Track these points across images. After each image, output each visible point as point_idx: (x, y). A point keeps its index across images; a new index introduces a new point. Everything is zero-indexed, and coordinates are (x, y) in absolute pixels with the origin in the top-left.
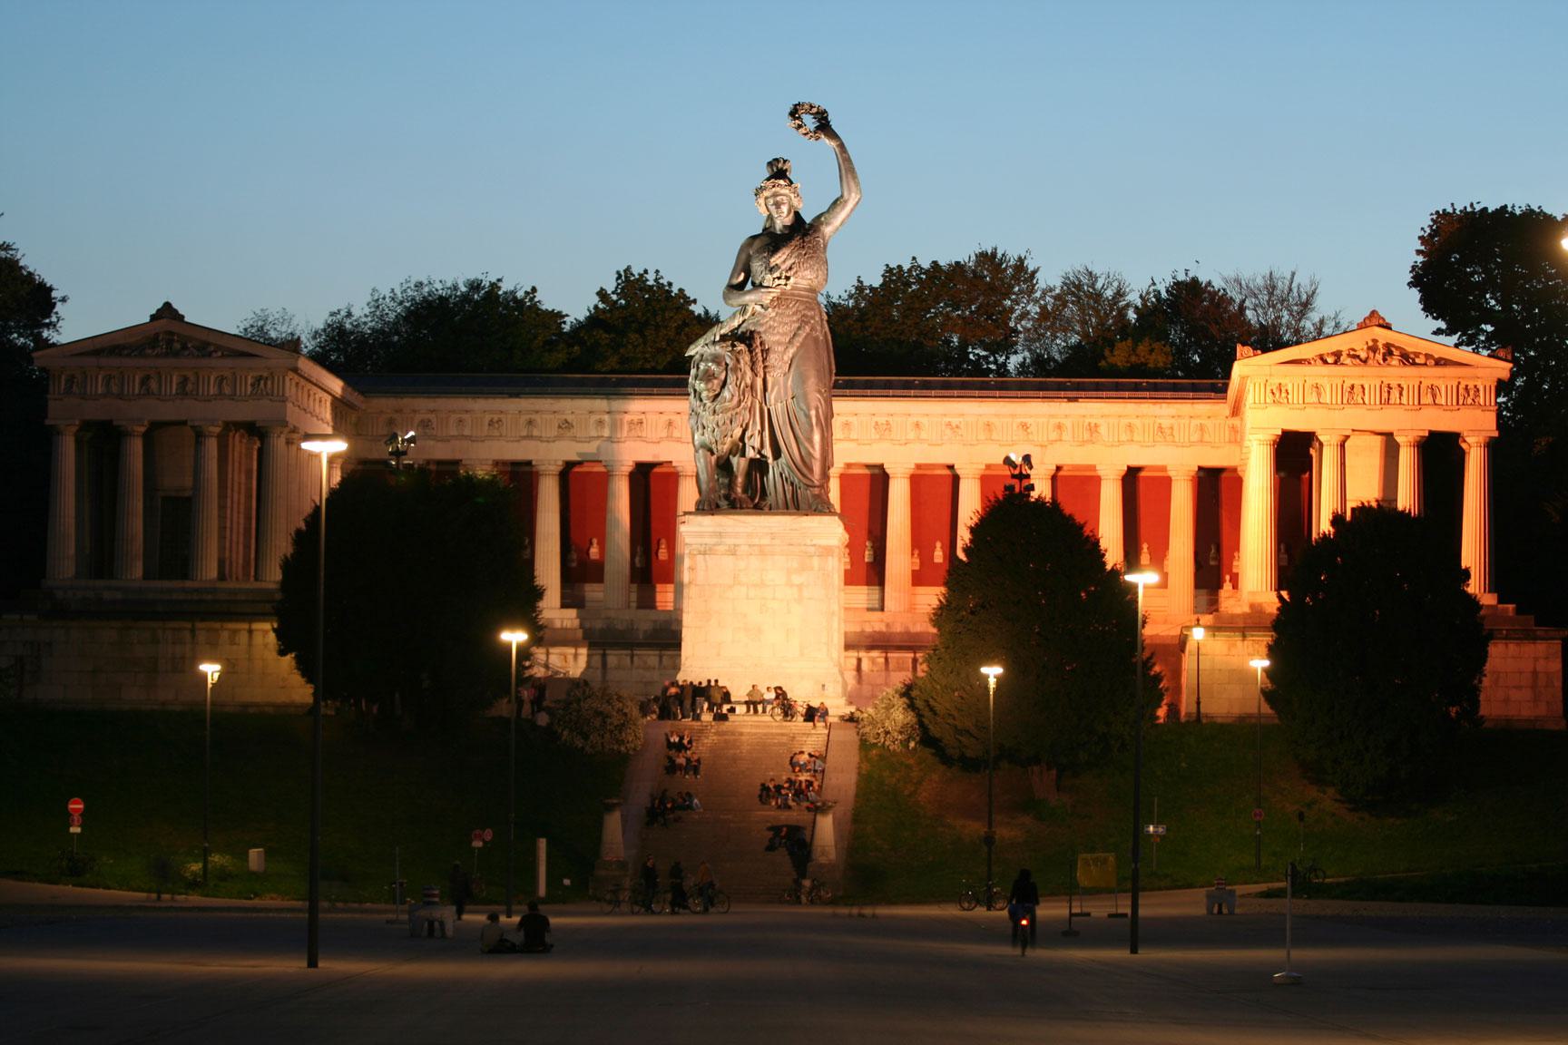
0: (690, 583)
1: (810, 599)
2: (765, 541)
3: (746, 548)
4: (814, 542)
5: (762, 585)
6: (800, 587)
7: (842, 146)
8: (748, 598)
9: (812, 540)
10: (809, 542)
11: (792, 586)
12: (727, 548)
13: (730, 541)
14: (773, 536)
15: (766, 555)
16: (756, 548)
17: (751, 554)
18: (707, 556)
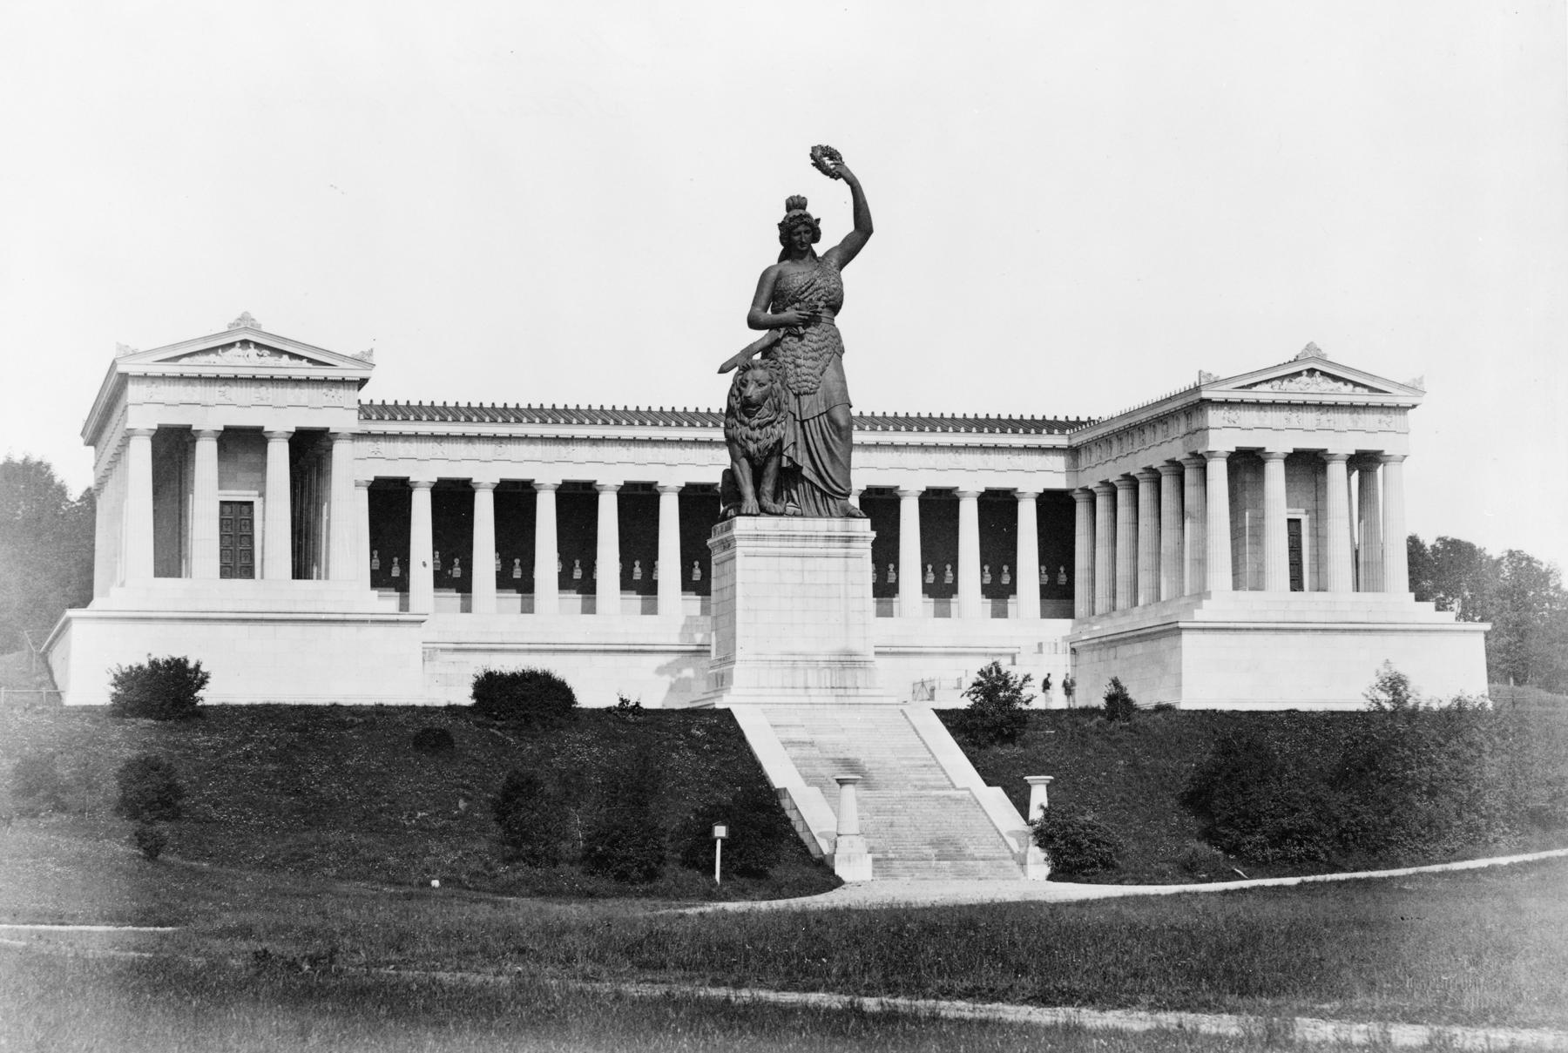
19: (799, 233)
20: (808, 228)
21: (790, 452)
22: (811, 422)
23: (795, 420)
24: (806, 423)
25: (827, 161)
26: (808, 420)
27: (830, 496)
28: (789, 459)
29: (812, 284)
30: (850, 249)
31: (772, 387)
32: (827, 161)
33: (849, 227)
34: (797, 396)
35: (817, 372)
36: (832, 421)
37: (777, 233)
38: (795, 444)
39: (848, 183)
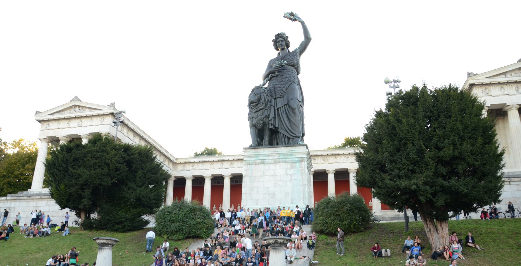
0: (245, 176)
1: (296, 180)
2: (277, 157)
3: (269, 160)
4: (297, 156)
5: (275, 175)
6: (291, 175)
7: (303, 23)
8: (269, 181)
9: (295, 155)
10: (294, 157)
11: (287, 175)
12: (260, 161)
13: (261, 158)
14: (279, 155)
15: (276, 163)
16: (272, 160)
17: (270, 163)
18: (252, 165)
19: (279, 41)
20: (283, 39)
21: (272, 122)
22: (282, 108)
23: (275, 109)
24: (279, 110)
25: (292, 17)
26: (280, 108)
27: (291, 138)
28: (272, 124)
29: (283, 58)
30: (303, 47)
31: (261, 96)
32: (292, 17)
33: (302, 39)
34: (275, 99)
35: (284, 89)
36: (290, 107)
37: (273, 43)
38: (275, 118)
39: (299, 21)
